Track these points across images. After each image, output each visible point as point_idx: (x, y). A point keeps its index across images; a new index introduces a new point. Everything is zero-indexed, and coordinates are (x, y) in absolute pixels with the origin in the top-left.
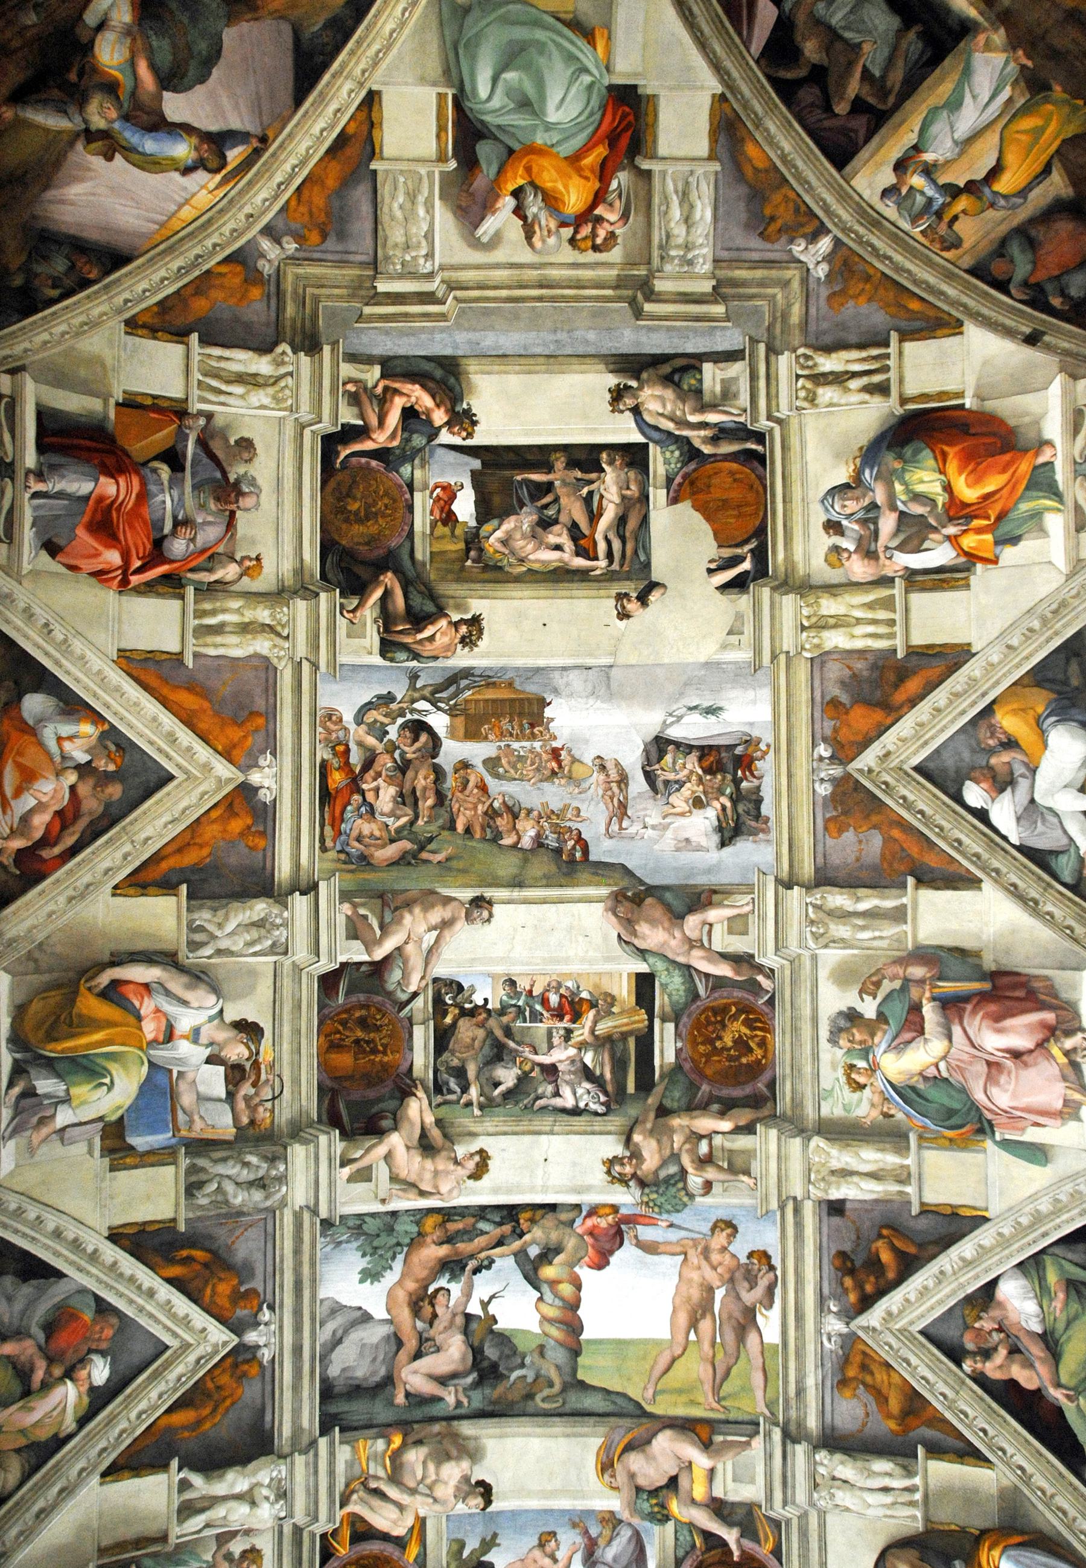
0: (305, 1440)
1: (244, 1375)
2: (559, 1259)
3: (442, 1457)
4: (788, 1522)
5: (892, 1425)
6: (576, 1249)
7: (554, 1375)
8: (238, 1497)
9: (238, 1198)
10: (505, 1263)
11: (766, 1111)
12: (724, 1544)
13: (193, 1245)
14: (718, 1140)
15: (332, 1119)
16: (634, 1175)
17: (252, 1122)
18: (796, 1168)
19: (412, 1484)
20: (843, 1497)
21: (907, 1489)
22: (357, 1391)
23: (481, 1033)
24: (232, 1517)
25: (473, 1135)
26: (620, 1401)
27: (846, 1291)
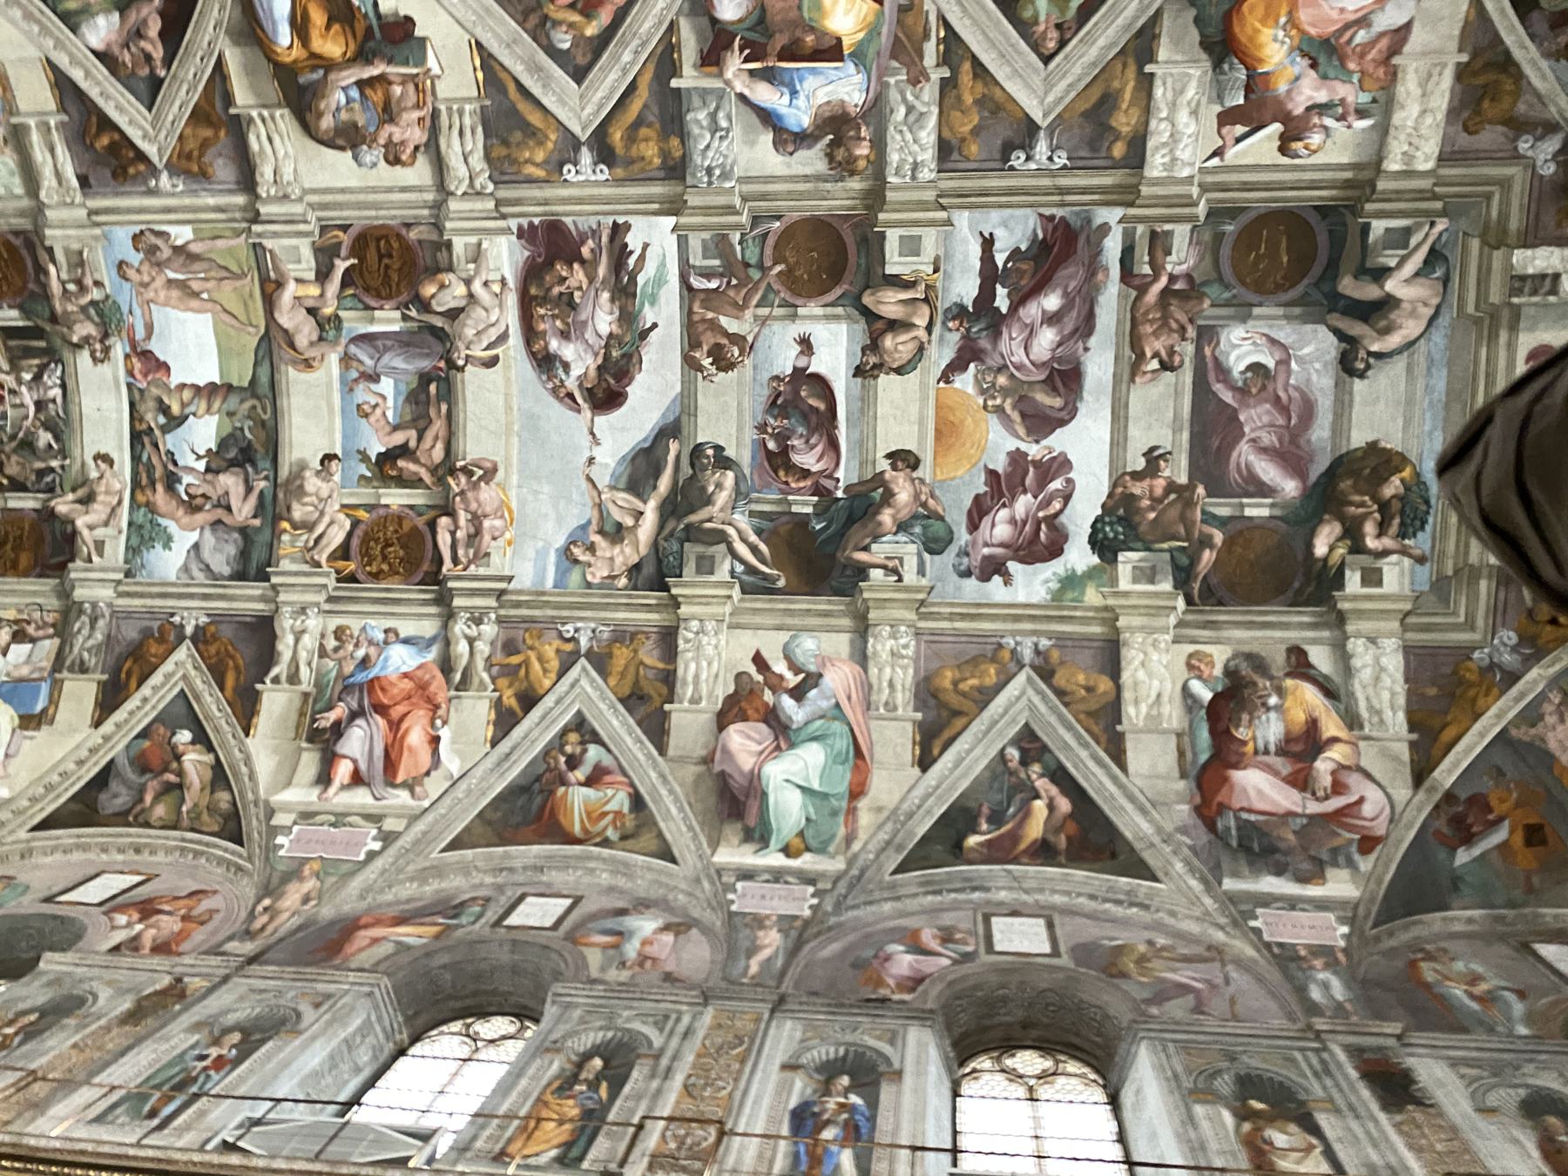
0: (270, 593)
1: (213, 635)
2: (166, 401)
3: (301, 492)
4: (319, 219)
5: (222, 133)
6: (157, 386)
7: (247, 405)
8: (297, 641)
9: (99, 636)
10: (170, 441)
11: (35, 239)
12: (347, 271)
13: (119, 670)
14: (64, 276)
15: (60, 569)
16: (102, 341)
17: (54, 625)
18: (65, 214)
19: (317, 514)
20: (287, 173)
21: (263, 120)
22: (244, 554)
23: (14, 458)
24: (309, 646)
25: (83, 464)
26: (261, 353)
27: (138, 173)
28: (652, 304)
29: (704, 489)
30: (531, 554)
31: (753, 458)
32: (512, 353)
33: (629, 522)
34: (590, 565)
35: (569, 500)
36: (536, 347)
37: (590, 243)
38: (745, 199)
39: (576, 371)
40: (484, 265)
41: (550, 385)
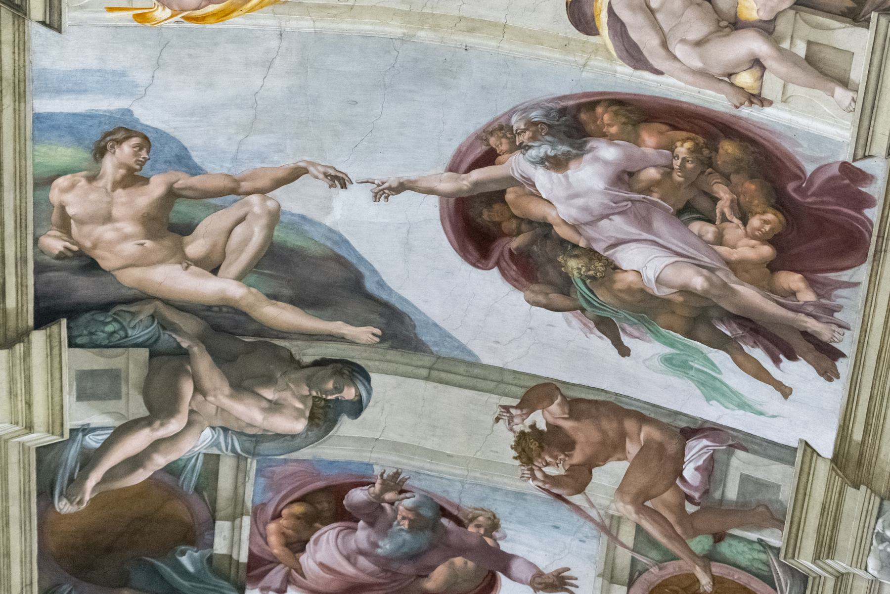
28: (668, 360)
29: (269, 380)
30: (117, 60)
31: (331, 463)
32: (598, 62)
33: (196, 247)
34: (92, 179)
35: (250, 128)
36: (605, 116)
37: (807, 296)
38: (840, 577)
39: (543, 179)
40: (796, 73)
41: (517, 123)
